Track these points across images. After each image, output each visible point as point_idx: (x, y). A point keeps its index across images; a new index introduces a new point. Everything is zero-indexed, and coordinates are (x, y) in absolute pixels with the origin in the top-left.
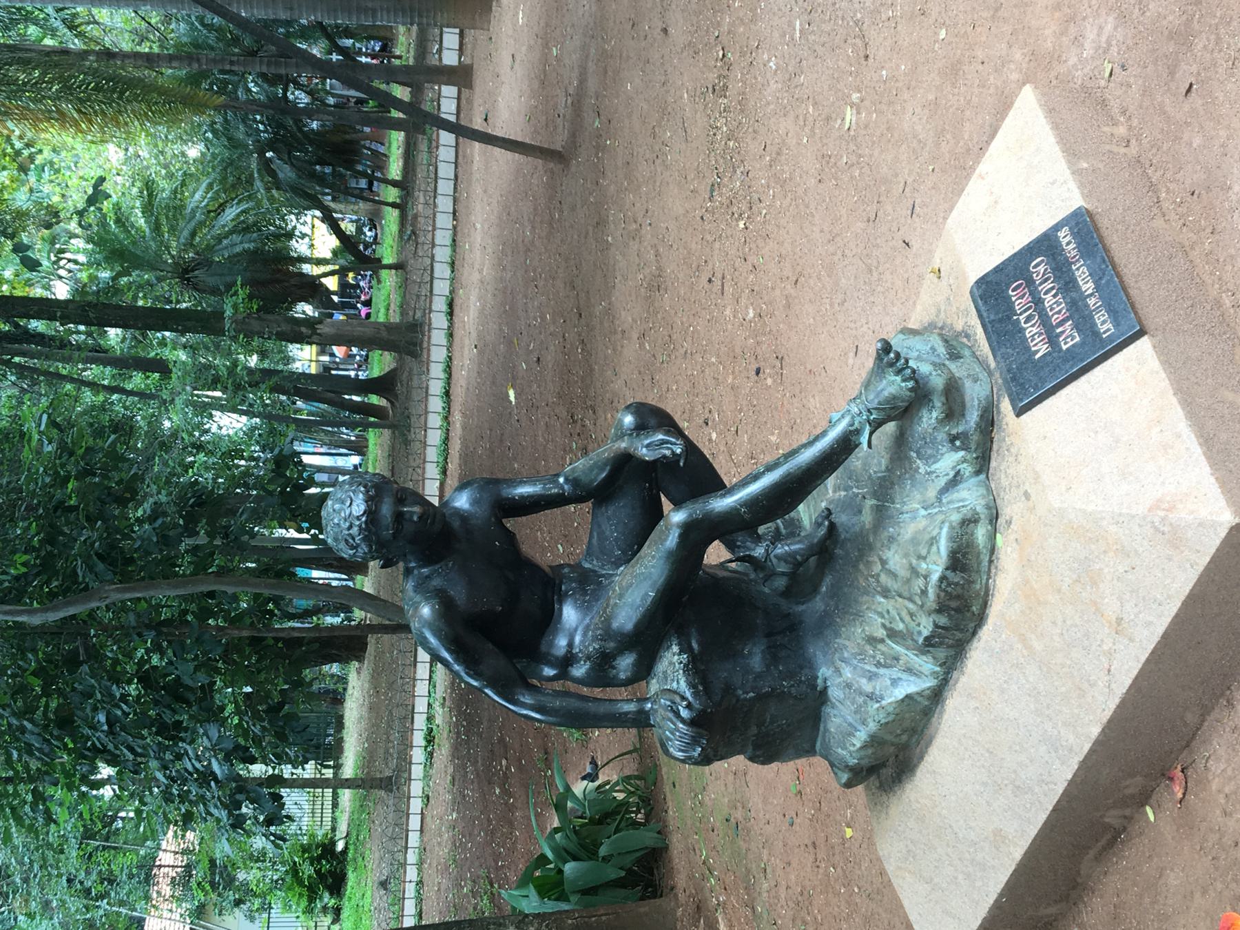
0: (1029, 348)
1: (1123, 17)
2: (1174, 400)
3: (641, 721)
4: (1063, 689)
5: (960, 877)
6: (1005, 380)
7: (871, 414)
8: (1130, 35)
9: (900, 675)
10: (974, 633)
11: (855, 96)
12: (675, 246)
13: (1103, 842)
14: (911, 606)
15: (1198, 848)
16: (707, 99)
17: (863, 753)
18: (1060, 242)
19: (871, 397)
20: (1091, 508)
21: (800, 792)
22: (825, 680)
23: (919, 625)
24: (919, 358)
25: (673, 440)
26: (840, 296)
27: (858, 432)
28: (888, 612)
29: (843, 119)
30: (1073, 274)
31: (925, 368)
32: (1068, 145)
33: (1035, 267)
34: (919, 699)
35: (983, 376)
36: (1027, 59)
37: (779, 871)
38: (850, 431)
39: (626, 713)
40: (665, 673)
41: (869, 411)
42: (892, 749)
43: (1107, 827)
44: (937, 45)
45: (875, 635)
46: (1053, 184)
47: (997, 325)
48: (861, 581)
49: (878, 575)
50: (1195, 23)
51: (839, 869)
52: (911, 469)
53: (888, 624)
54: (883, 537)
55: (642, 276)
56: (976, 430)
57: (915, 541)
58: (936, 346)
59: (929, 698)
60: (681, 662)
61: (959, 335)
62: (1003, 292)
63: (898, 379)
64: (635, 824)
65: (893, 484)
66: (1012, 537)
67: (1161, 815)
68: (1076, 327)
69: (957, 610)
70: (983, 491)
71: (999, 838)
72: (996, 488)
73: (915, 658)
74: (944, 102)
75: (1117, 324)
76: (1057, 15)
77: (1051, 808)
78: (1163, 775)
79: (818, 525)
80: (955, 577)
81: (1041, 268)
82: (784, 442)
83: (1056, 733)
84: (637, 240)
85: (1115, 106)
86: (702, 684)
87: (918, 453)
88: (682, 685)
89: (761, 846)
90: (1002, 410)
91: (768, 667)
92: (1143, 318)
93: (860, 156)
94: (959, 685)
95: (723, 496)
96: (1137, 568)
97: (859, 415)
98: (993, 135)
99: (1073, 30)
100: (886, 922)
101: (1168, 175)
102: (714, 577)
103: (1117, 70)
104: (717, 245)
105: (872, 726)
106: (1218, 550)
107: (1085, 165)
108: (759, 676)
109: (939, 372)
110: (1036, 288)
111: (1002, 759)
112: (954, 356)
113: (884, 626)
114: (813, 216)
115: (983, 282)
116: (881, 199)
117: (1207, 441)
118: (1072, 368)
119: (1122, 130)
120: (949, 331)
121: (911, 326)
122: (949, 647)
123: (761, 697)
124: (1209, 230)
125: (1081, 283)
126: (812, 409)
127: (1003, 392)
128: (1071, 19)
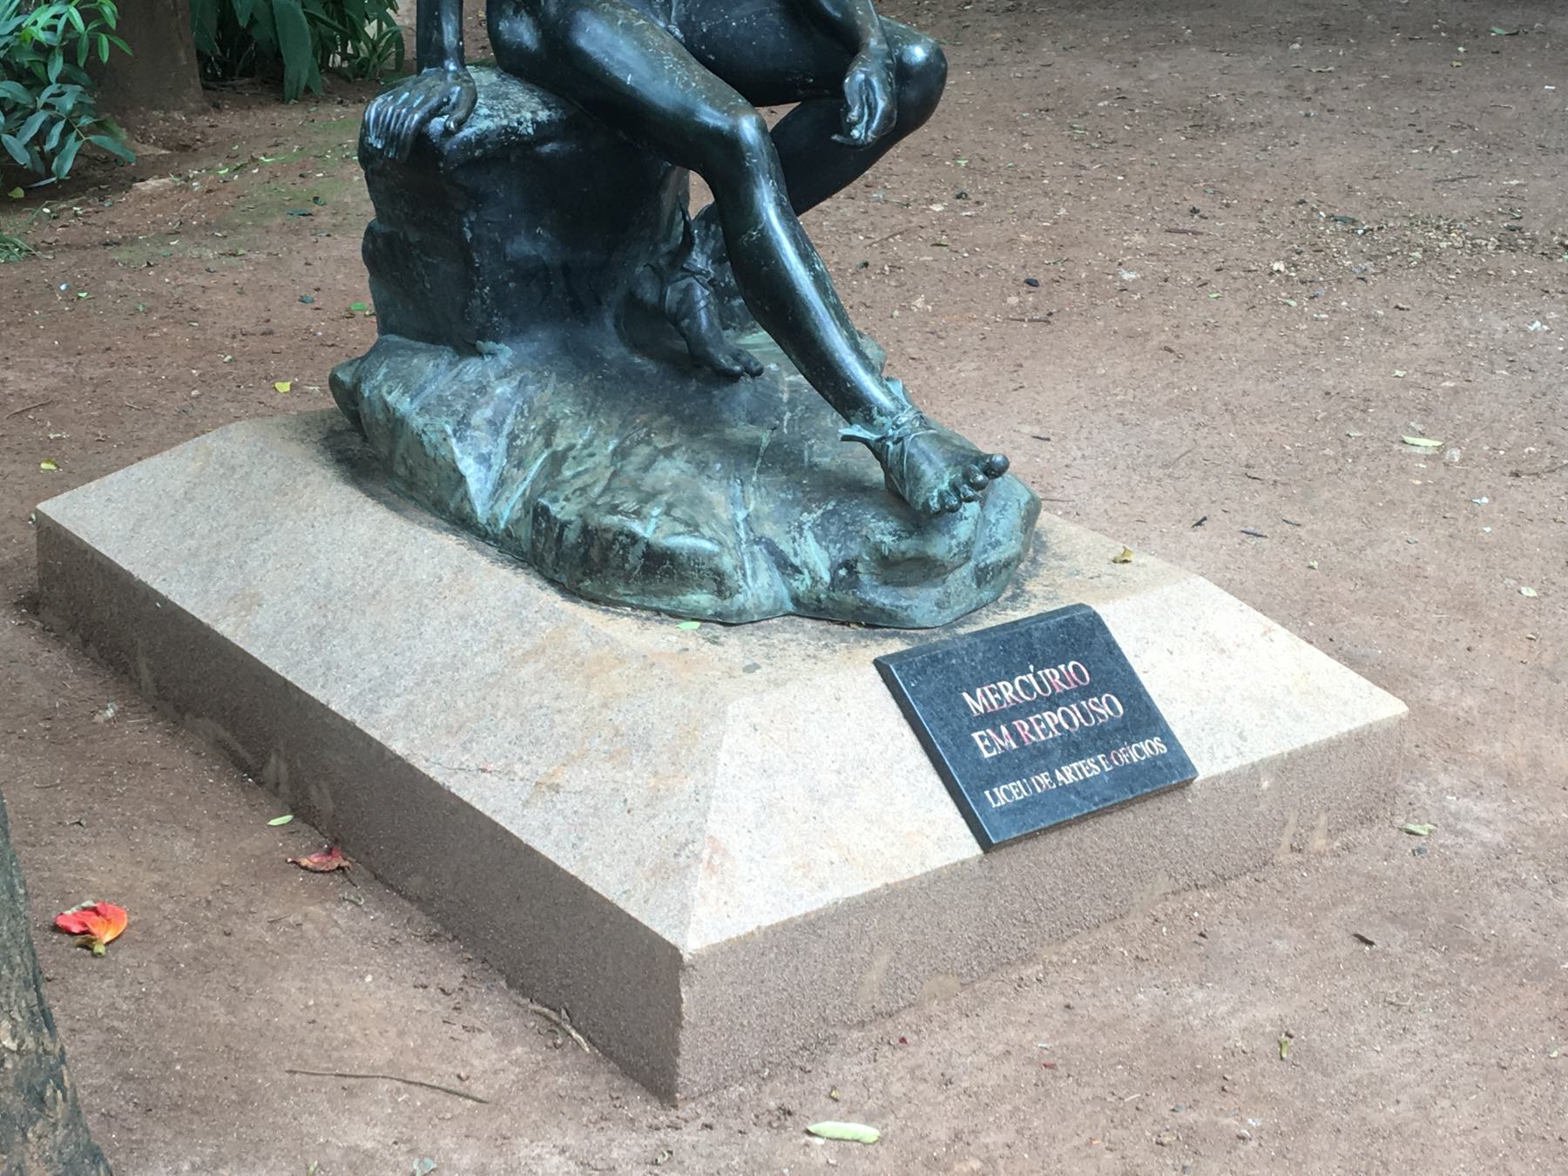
0: (981, 686)
1: (1499, 854)
2: (878, 884)
3: (431, 53)
4: (461, 704)
5: (193, 543)
6: (936, 646)
7: (895, 443)
8: (1467, 863)
9: (496, 468)
10: (552, 582)
11: (1455, 454)
12: (1262, 156)
13: (242, 752)
14: (597, 490)
15: (225, 883)
16: (1502, 218)
17: (378, 406)
18: (1143, 740)
19: (922, 444)
20: (723, 756)
21: (352, 316)
22: (492, 354)
23: (567, 499)
24: (983, 520)
25: (874, 125)
26: (1132, 418)
27: (868, 422)
28: (592, 455)
29: (1422, 434)
30: (1090, 756)
31: (963, 530)
32: (1301, 761)
33: (1109, 702)
34: (458, 495)
35: (947, 616)
36: (1461, 714)
37: (230, 278)
38: (870, 409)
39: (440, 32)
40: (506, 96)
41: (900, 439)
42: (384, 450)
43: (263, 759)
44: (1513, 582)
45: (558, 434)
46: (1241, 736)
47: (1022, 641)
48: (644, 417)
49: (649, 443)
50: (1467, 955)
51: (228, 369)
52: (809, 500)
53: (573, 453)
54: (708, 452)
55: (1223, 98)
56: (862, 600)
57: (697, 500)
58: (1001, 549)
59: (458, 509)
60: (520, 123)
61: (1019, 584)
62: (1076, 652)
63: (945, 486)
64: (324, 49)
65: (789, 472)
66: (691, 644)
67: (278, 834)
68: (1006, 754)
69: (586, 558)
70: (767, 605)
71: (249, 602)
72: (771, 626)
73: (520, 492)
74: (1418, 589)
75: (1003, 811)
76: (1522, 761)
77: (289, 678)
78: (336, 841)
79: (736, 358)
80: (634, 558)
81: (1105, 711)
82: (911, 319)
83: (397, 691)
84: (1285, 93)
85: (1363, 835)
86: (483, 155)
87: (833, 512)
88: (483, 123)
89: (271, 250)
90: (890, 641)
91: (513, 264)
92: (1010, 850)
93: (1356, 458)
94: (476, 556)
95: (779, 203)
96: (628, 817)
97: (894, 423)
98: (1352, 662)
99: (1492, 783)
100: (141, 434)
101: (1238, 904)
102: (661, 184)
103: (1416, 842)
104: (1253, 225)
105: (418, 422)
106: (646, 928)
107: (1265, 785)
108: (498, 249)
109: (956, 550)
110: (1074, 701)
111: (364, 612)
112: (982, 576)
113: (571, 447)
114: (1272, 381)
115: (1095, 624)
116: (1280, 488)
117: (811, 925)
118: (943, 744)
119: (1319, 842)
120: (1027, 571)
121: (1044, 519)
122: (533, 543)
123: (464, 252)
124: (1142, 954)
125: (1074, 765)
126: (958, 366)
127: (917, 643)
128: (1511, 779)
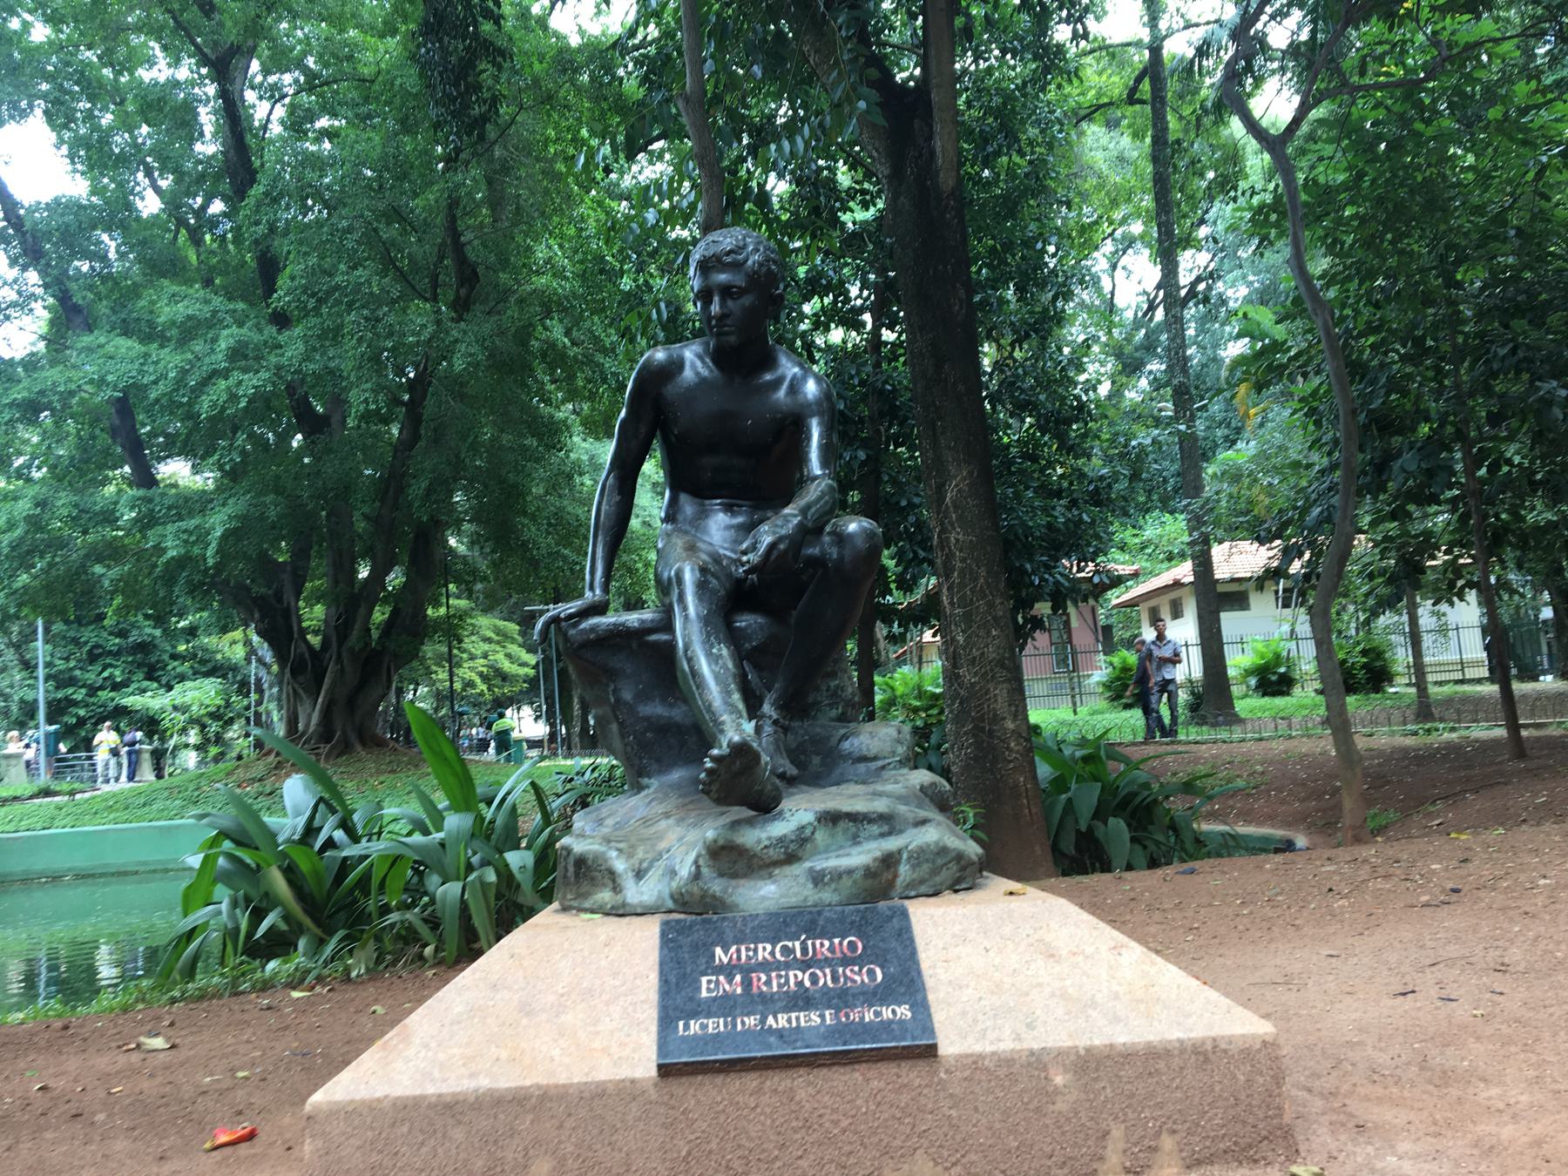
2: (528, 1083)
68: (726, 996)
91: (647, 719)
125: (793, 1015)
